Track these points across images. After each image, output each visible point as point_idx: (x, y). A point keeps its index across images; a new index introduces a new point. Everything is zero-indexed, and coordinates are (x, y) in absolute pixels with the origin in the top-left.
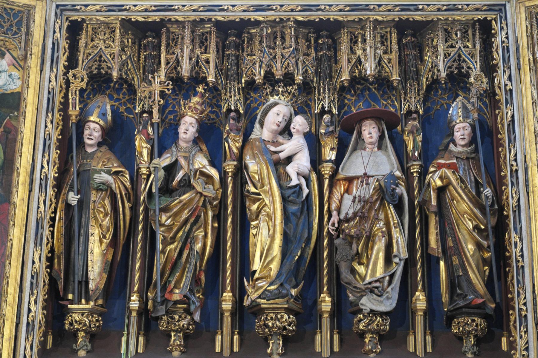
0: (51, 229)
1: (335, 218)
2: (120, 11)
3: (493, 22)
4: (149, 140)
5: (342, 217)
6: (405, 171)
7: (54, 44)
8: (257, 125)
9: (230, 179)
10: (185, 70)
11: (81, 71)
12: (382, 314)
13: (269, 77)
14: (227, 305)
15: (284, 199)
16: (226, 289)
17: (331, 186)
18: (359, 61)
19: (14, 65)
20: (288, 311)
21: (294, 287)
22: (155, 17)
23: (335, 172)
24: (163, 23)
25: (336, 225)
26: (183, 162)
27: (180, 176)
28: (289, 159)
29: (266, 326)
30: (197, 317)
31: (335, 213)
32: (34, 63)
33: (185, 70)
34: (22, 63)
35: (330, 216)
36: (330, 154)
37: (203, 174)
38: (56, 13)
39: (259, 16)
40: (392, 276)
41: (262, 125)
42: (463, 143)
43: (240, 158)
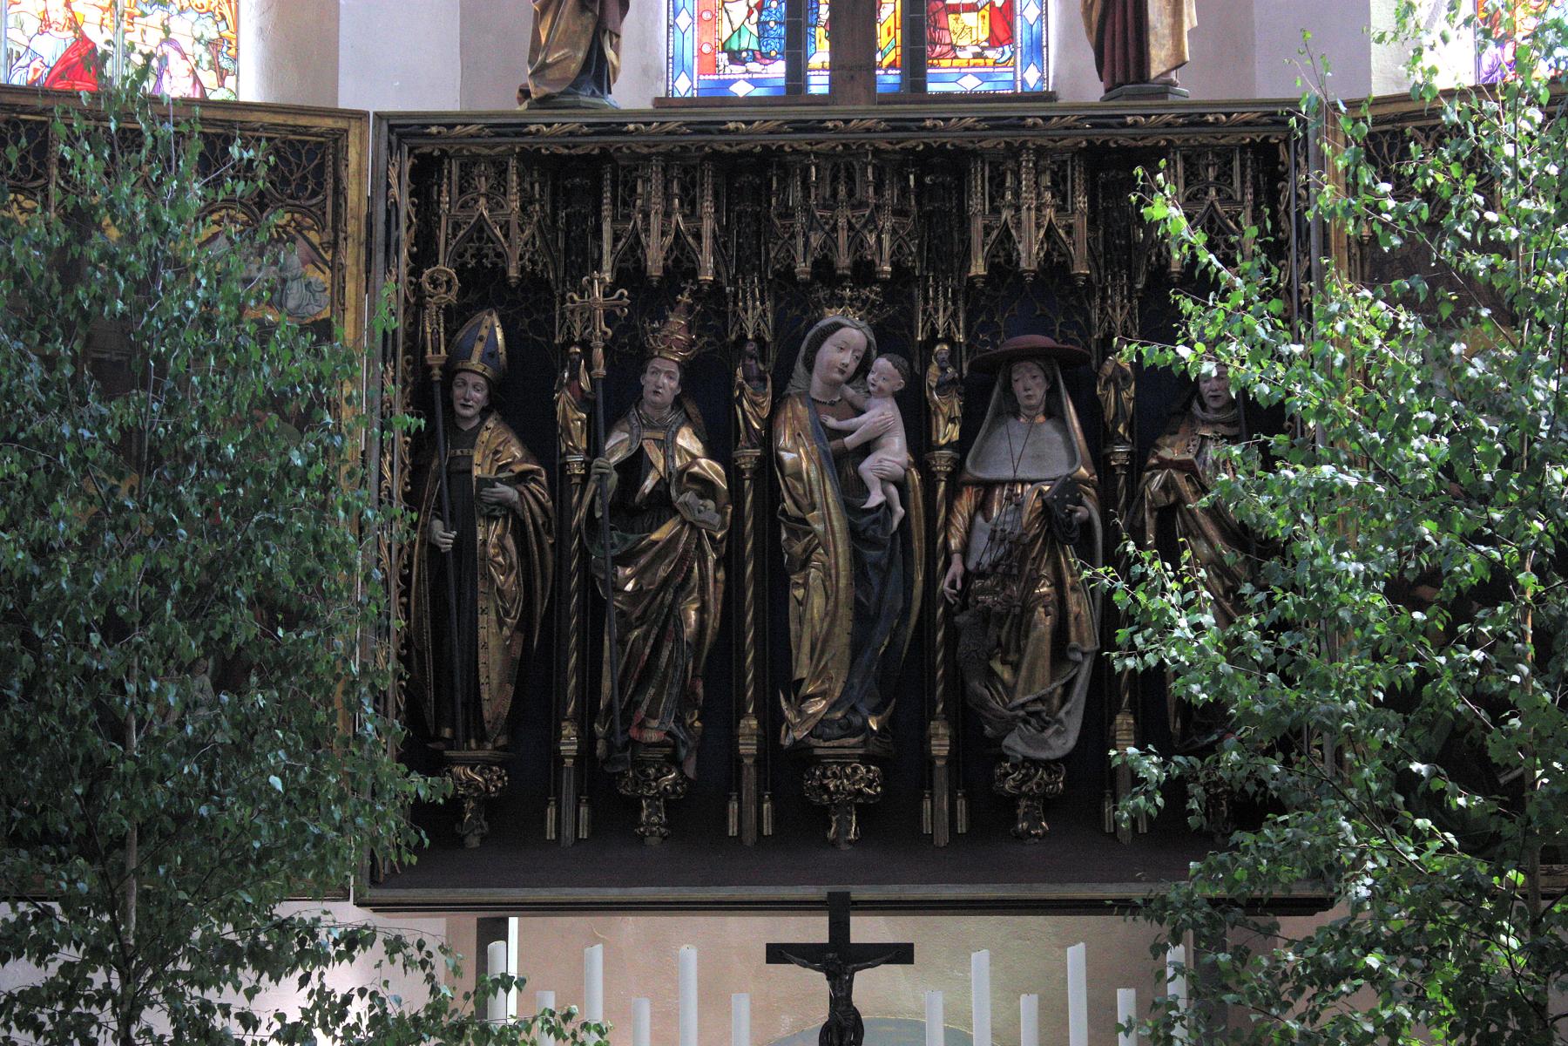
0: (404, 600)
1: (956, 568)
2: (517, 135)
3: (1282, 147)
4: (585, 402)
5: (971, 566)
6: (1100, 461)
7: (388, 212)
8: (799, 367)
9: (747, 483)
10: (655, 258)
11: (444, 267)
12: (1047, 764)
13: (824, 268)
14: (748, 748)
15: (854, 534)
16: (745, 711)
17: (953, 493)
18: (1006, 235)
19: (313, 263)
20: (866, 760)
21: (875, 711)
22: (592, 146)
23: (958, 466)
24: (605, 155)
25: (959, 586)
26: (656, 456)
27: (649, 484)
28: (867, 448)
29: (826, 789)
30: (690, 771)
31: (957, 559)
32: (351, 256)
33: (655, 258)
34: (328, 257)
36: (948, 432)
37: (695, 478)
38: (390, 143)
39: (800, 141)
40: (1068, 687)
41: (810, 365)
42: (1215, 405)
43: (767, 440)
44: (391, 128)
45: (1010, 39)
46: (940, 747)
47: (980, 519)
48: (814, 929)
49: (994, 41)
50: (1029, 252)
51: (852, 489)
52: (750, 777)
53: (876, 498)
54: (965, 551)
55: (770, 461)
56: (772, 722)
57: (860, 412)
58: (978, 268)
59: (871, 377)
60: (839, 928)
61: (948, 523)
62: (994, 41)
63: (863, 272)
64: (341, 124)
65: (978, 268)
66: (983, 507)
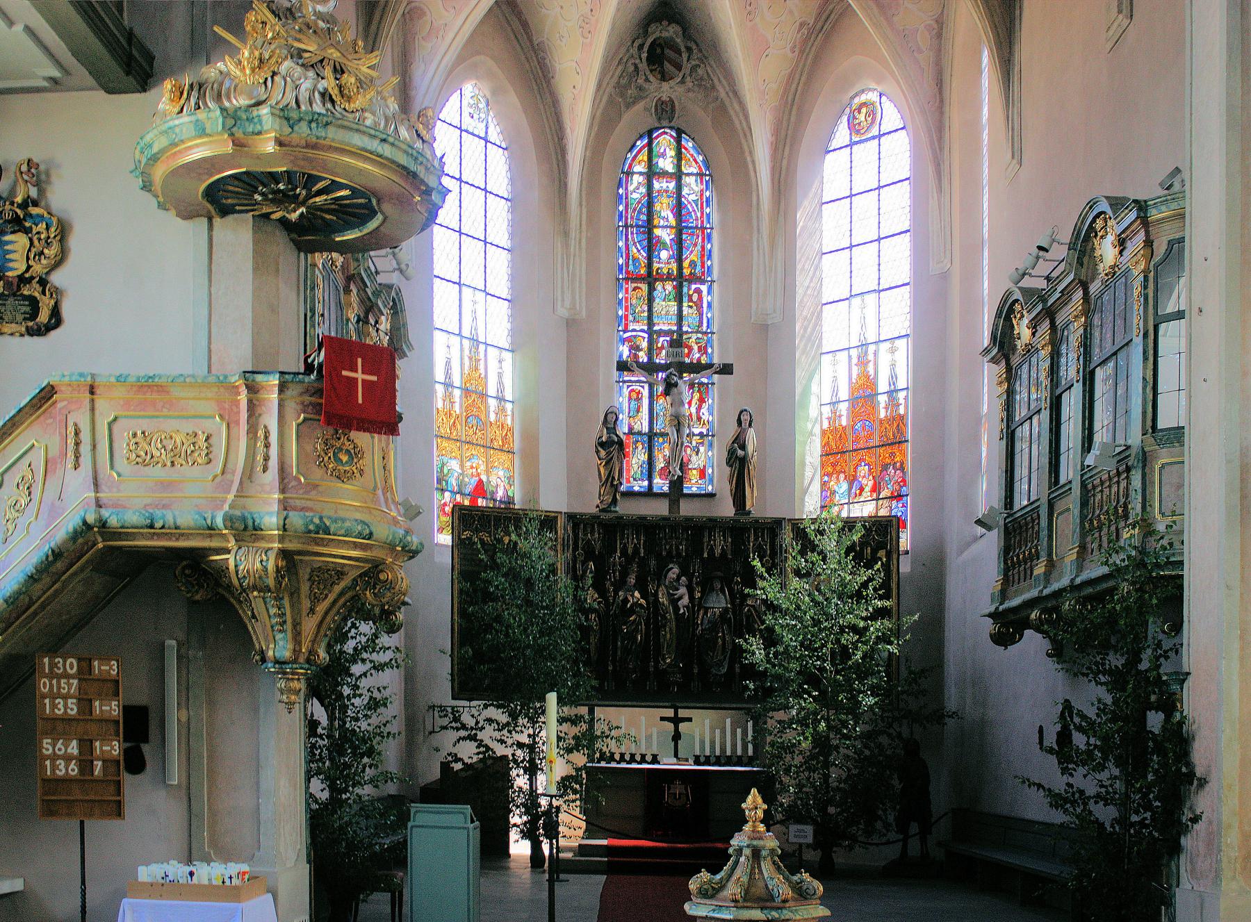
13: (669, 553)
17: (699, 610)
36: (698, 595)
45: (704, 477)
49: (701, 478)
50: (718, 551)
51: (676, 608)
53: (682, 611)
57: (678, 589)
62: (701, 478)
63: (679, 554)
66: (706, 613)
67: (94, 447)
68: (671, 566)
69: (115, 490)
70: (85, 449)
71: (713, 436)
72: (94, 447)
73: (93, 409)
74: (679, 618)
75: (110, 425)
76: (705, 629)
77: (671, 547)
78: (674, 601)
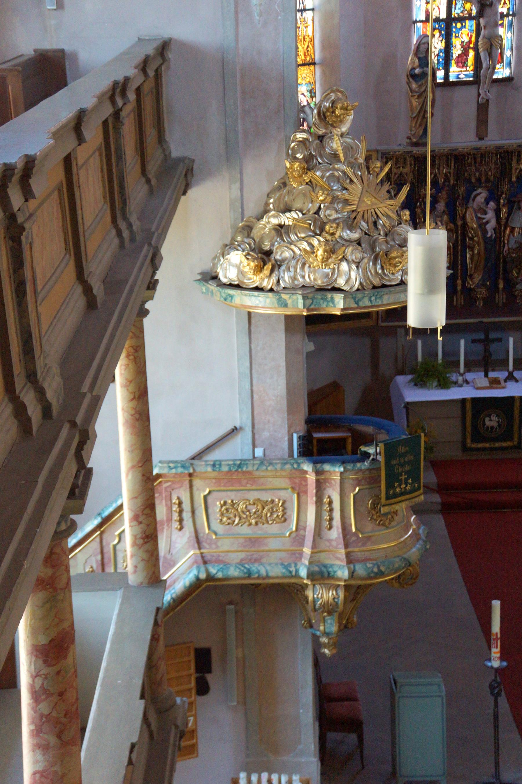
8: (471, 201)
13: (479, 180)
14: (459, 287)
15: (486, 242)
17: (505, 229)
28: (487, 222)
31: (506, 245)
33: (441, 181)
35: (504, 247)
41: (474, 200)
43: (464, 218)
44: (382, 153)
46: (501, 286)
47: (511, 236)
48: (482, 336)
51: (485, 232)
52: (459, 293)
53: (489, 235)
54: (508, 243)
55: (465, 224)
56: (464, 281)
57: (486, 213)
58: (514, 179)
59: (489, 206)
60: (487, 336)
61: (504, 236)
63: (488, 180)
64: (371, 153)
65: (514, 179)
67: (193, 512)
68: (480, 190)
69: (214, 546)
70: (187, 515)
71: (514, 15)
72: (193, 512)
73: (191, 487)
74: (486, 241)
75: (205, 497)
76: (512, 249)
77: (480, 174)
78: (482, 226)
